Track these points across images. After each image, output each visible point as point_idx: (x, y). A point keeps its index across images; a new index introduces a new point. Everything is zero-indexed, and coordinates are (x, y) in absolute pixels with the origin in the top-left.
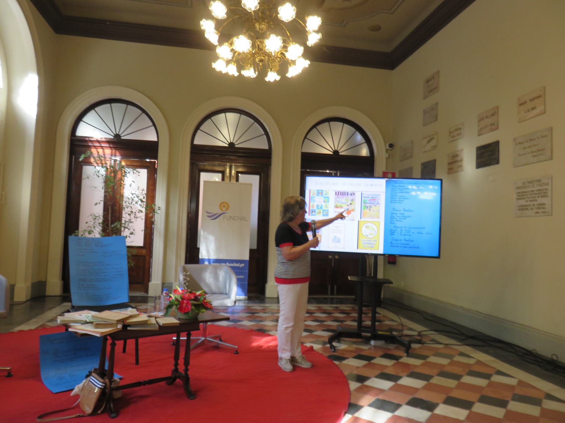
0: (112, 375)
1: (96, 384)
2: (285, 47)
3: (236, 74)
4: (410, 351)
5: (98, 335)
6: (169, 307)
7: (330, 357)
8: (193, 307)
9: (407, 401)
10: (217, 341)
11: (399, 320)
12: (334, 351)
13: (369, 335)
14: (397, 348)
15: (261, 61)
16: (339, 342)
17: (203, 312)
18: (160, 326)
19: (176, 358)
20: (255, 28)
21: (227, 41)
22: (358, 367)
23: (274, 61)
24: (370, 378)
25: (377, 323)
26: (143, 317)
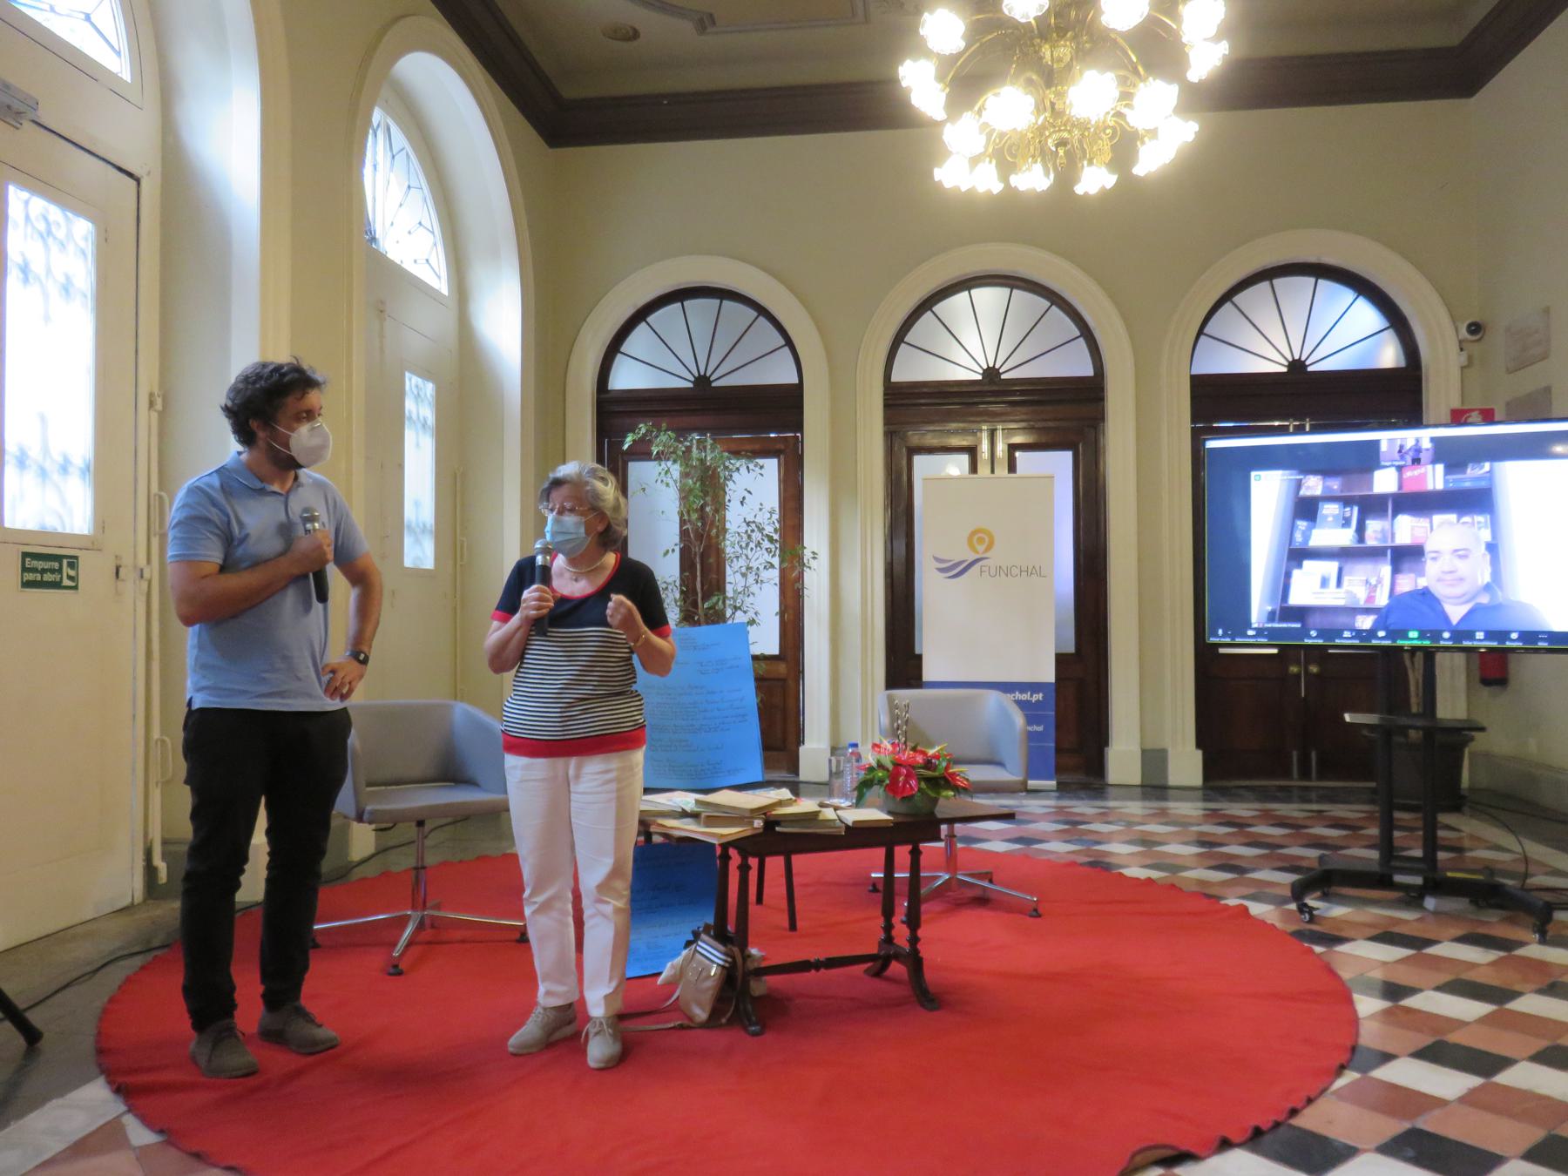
0: (743, 946)
1: (712, 957)
2: (1126, 96)
3: (997, 187)
4: (1551, 930)
5: (715, 842)
6: (864, 786)
7: (1299, 935)
8: (923, 785)
9: (1533, 1052)
10: (986, 884)
11: (1518, 849)
12: (1312, 920)
13: (1418, 880)
14: (1511, 921)
15: (1062, 143)
16: (1325, 897)
17: (947, 798)
18: (847, 827)
19: (888, 913)
20: (1041, 58)
21: (969, 105)
22: (1385, 963)
23: (1096, 137)
24: (1421, 990)
25: (1441, 855)
26: (806, 805)
